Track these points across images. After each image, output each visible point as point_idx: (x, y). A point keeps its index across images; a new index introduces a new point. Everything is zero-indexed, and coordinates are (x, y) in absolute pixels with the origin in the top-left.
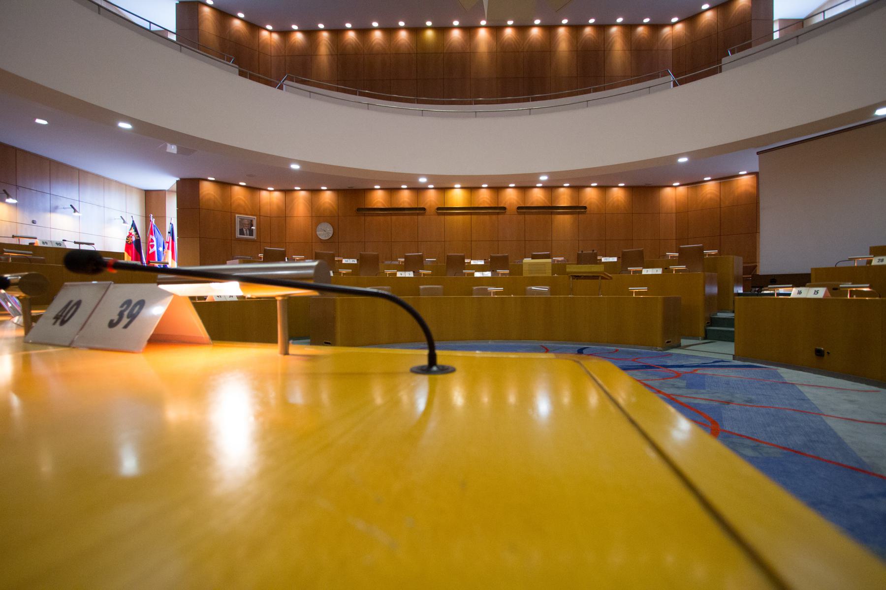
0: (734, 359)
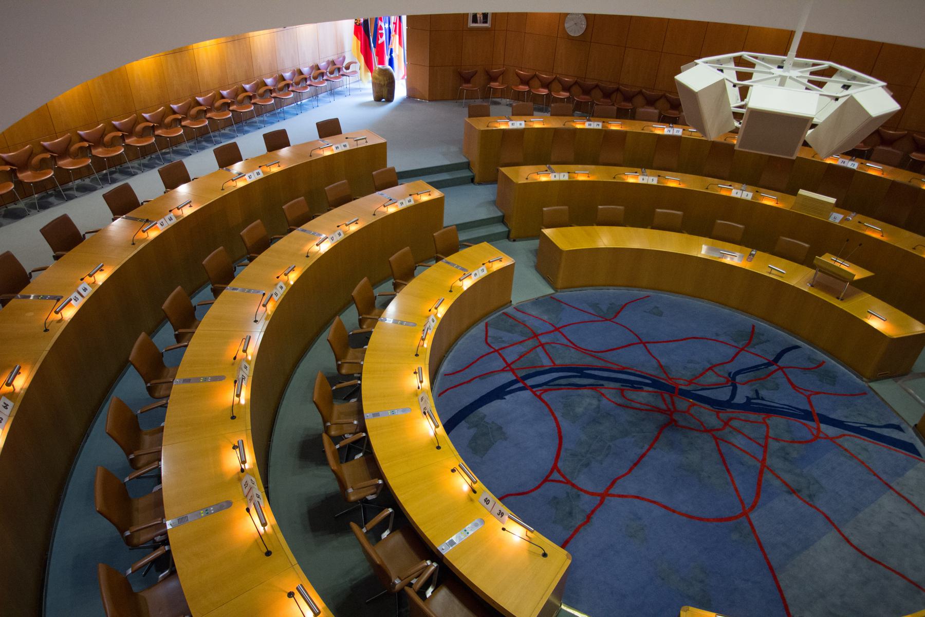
0: (913, 428)
